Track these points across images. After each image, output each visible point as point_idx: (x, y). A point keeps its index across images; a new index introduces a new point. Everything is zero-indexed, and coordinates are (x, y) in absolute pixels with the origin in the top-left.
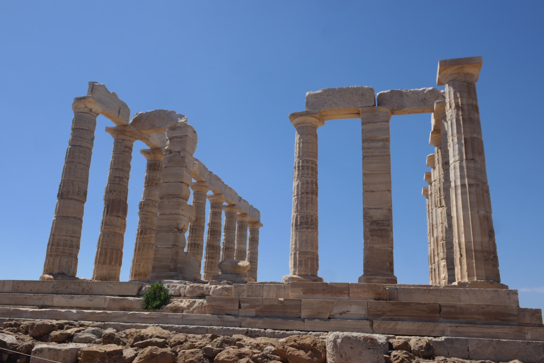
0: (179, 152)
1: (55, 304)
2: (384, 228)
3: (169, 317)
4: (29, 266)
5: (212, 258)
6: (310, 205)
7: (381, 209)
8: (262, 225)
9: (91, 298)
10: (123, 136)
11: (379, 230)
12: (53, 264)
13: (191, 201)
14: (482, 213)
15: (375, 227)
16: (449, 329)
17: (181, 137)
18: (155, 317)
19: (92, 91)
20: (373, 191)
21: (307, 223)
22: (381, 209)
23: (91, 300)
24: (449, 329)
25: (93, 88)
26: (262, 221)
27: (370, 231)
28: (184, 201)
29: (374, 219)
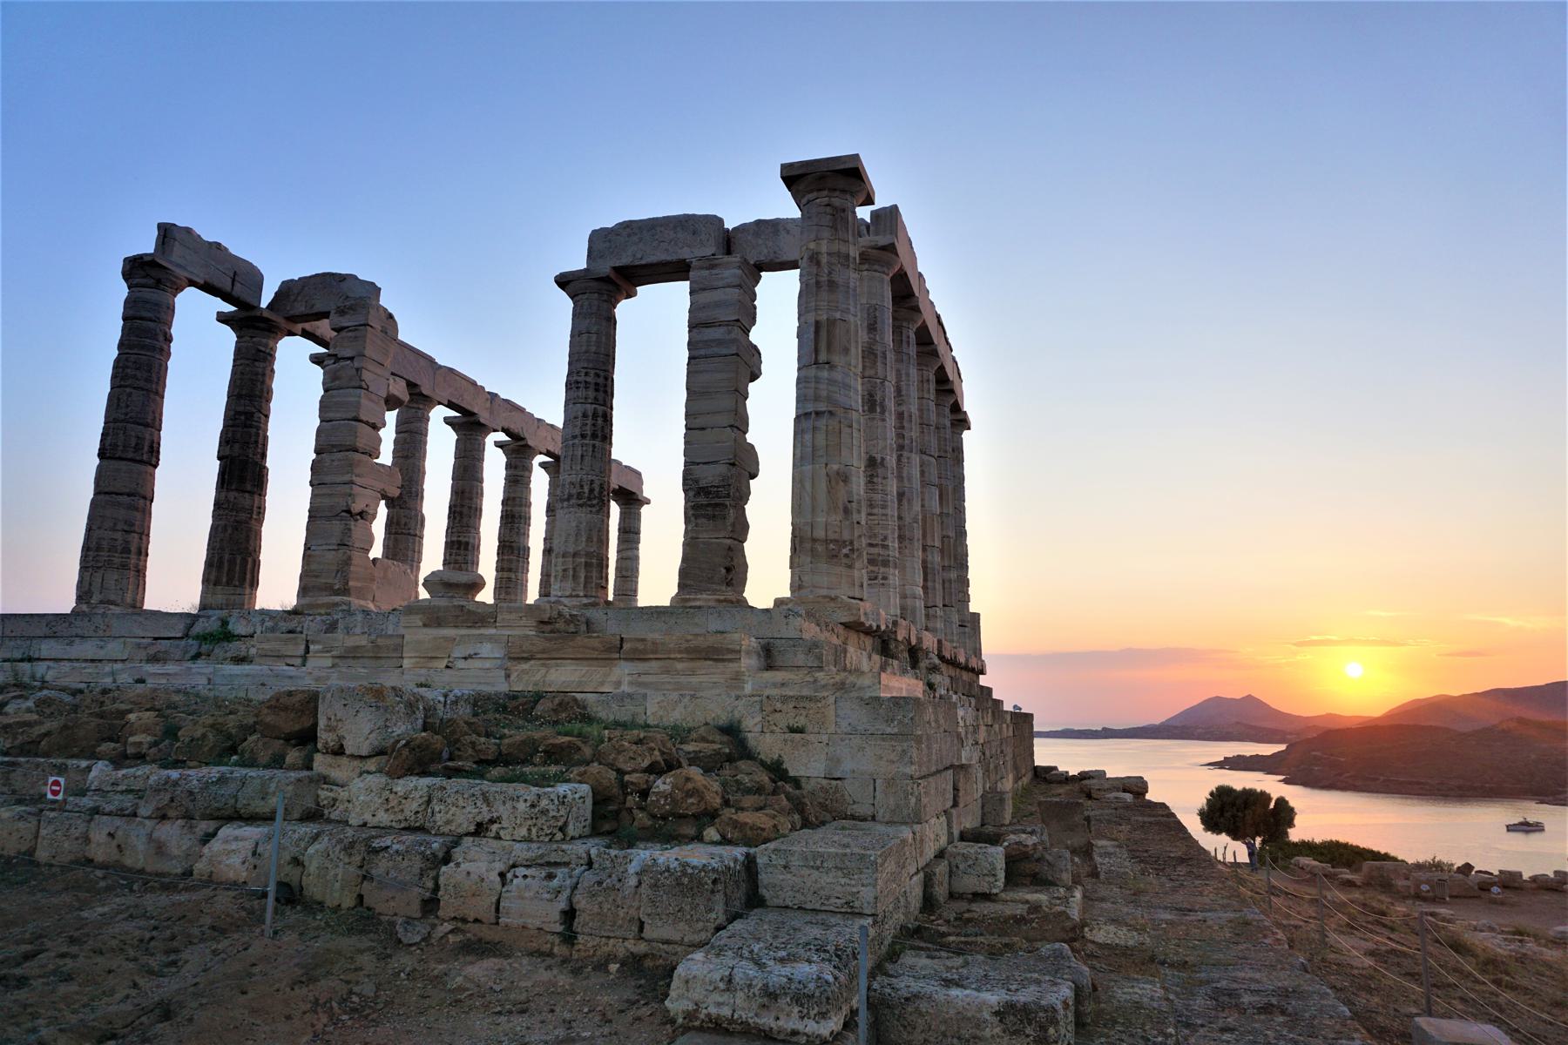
0: (351, 359)
2: (717, 501)
4: (56, 590)
5: (510, 570)
6: (587, 459)
8: (648, 502)
10: (256, 330)
13: (386, 457)
14: (835, 467)
16: (627, 679)
17: (356, 328)
21: (579, 496)
24: (627, 679)
26: (645, 494)
28: (365, 457)
29: (703, 484)
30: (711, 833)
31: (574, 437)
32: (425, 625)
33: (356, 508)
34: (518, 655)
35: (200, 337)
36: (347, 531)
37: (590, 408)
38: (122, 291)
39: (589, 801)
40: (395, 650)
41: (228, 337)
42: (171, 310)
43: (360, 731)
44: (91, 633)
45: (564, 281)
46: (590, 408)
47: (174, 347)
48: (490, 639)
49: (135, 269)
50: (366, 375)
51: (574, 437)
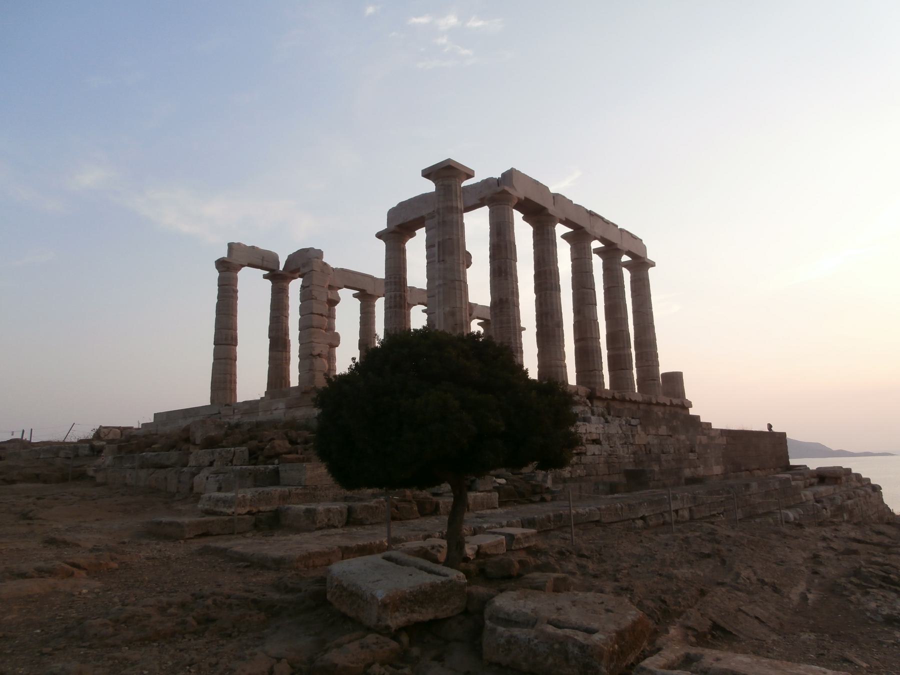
14: (447, 309)
30: (276, 461)
33: (316, 352)
34: (289, 407)
35: (254, 287)
36: (312, 364)
37: (393, 293)
38: (216, 274)
39: (247, 453)
41: (268, 284)
42: (236, 279)
43: (198, 436)
45: (379, 236)
46: (393, 293)
47: (239, 294)
49: (221, 264)
50: (315, 293)
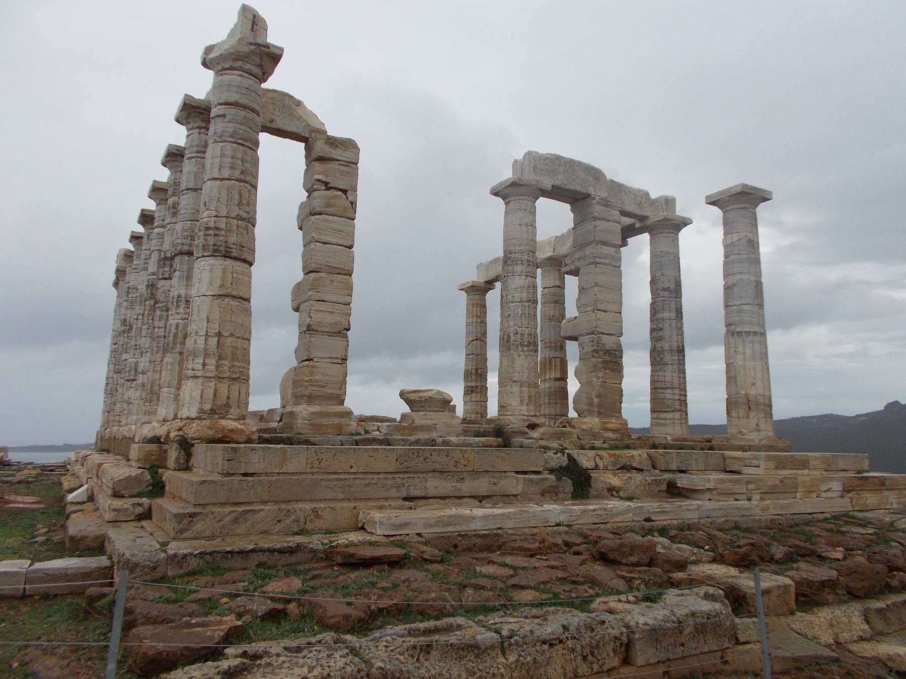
0: (345, 191)
1: (431, 492)
3: (684, 508)
7: (613, 335)
9: (495, 480)
11: (611, 362)
12: (228, 398)
15: (607, 358)
18: (667, 510)
19: (252, 30)
20: (605, 311)
22: (613, 335)
23: (495, 484)
25: (254, 23)
27: (603, 362)
29: (607, 347)
31: (530, 301)
32: (776, 468)
40: (794, 487)
44: (454, 469)
48: (836, 479)
51: (530, 301)
